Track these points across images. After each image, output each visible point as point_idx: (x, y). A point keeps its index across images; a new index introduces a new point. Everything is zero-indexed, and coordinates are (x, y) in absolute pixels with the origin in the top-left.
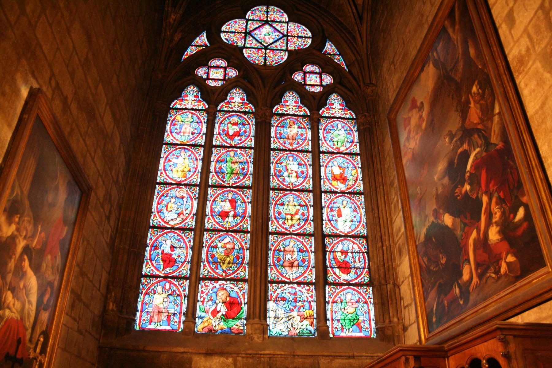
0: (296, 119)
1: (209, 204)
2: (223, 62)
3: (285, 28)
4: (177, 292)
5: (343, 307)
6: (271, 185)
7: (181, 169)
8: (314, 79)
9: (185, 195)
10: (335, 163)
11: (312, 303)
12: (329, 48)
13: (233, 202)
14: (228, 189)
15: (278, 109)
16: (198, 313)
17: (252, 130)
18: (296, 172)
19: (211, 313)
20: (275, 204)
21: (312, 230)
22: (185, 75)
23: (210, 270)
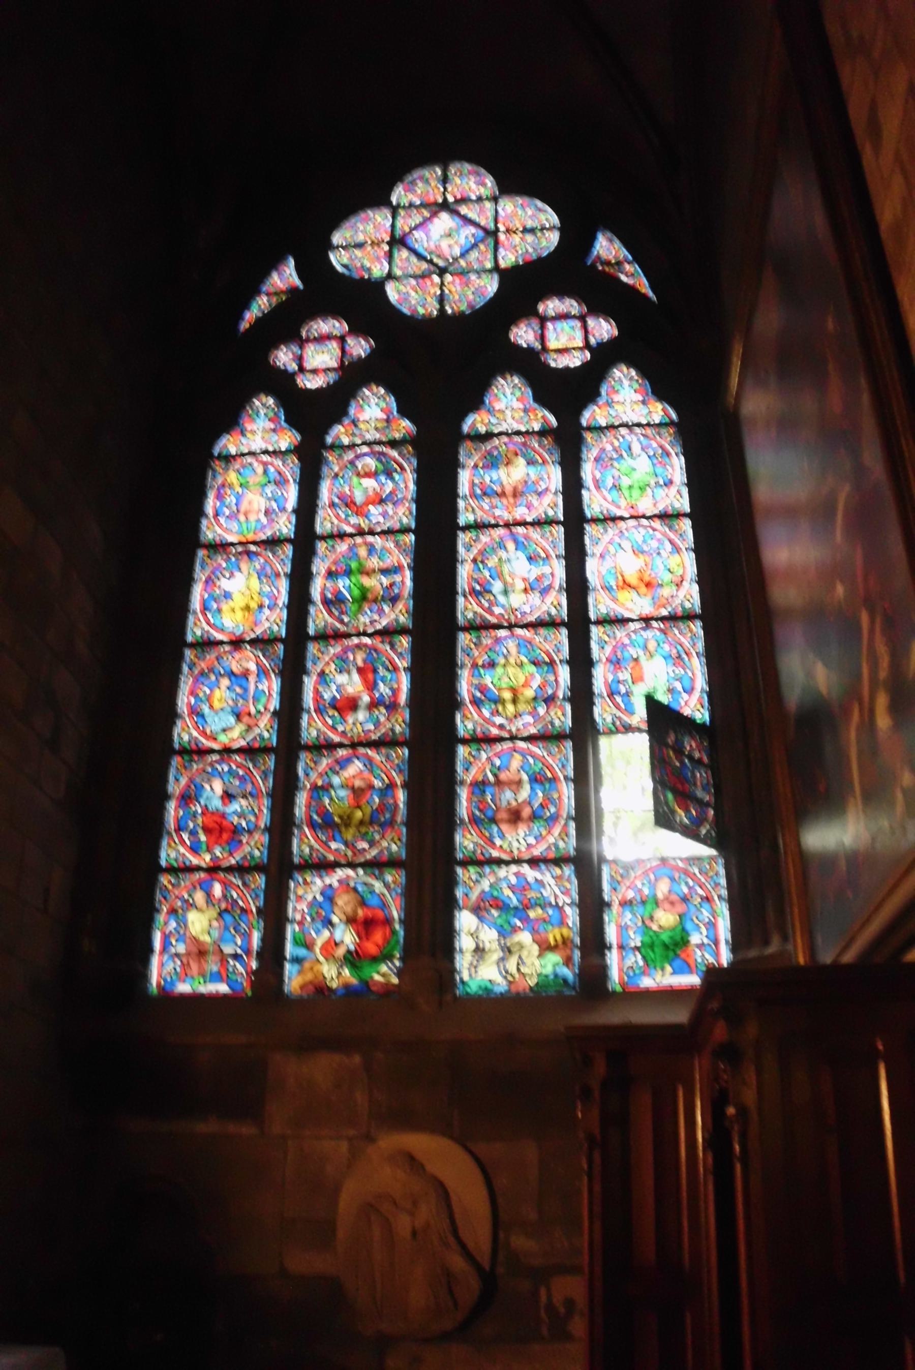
0: (524, 444)
1: (309, 683)
2: (337, 324)
3: (490, 214)
4: (241, 903)
5: (647, 915)
6: (461, 620)
7: (243, 604)
8: (565, 334)
9: (252, 667)
10: (626, 545)
11: (568, 910)
12: (606, 247)
13: (368, 672)
14: (356, 640)
15: (475, 422)
16: (290, 949)
17: (407, 483)
18: (524, 580)
19: (322, 949)
20: (475, 665)
21: (569, 722)
22: (242, 372)
23: (316, 846)
